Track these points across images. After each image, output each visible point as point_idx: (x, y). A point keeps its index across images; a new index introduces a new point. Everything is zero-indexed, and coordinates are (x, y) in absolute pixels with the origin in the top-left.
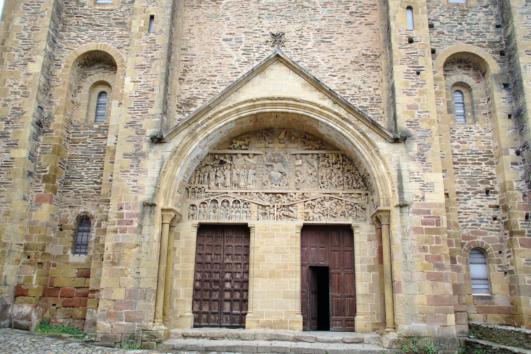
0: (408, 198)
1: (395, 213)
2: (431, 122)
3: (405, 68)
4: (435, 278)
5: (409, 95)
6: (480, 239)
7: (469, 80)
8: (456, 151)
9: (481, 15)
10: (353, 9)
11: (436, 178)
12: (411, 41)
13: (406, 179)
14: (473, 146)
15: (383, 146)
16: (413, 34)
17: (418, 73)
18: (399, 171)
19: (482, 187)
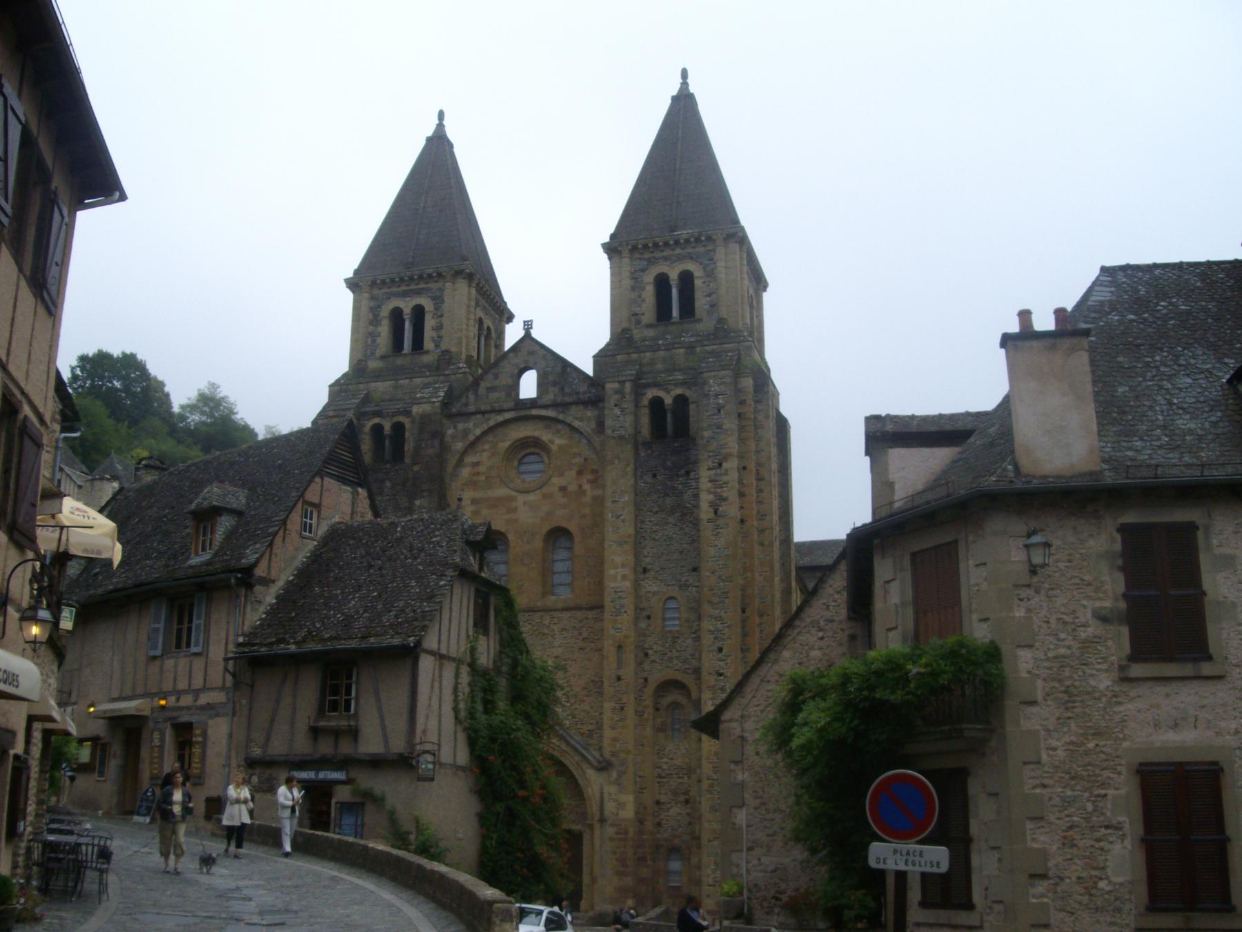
0: (606, 814)
1: (597, 826)
2: (628, 752)
3: (613, 704)
4: (620, 874)
5: (613, 728)
6: (677, 841)
7: (682, 699)
8: (665, 767)
9: (689, 641)
10: (585, 635)
11: (629, 799)
12: (619, 679)
13: (606, 800)
14: (678, 762)
15: (591, 773)
16: (621, 672)
17: (622, 709)
18: (602, 793)
19: (682, 798)
